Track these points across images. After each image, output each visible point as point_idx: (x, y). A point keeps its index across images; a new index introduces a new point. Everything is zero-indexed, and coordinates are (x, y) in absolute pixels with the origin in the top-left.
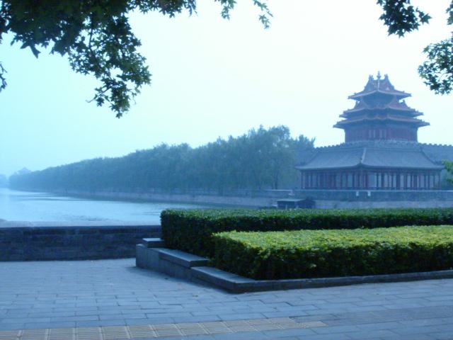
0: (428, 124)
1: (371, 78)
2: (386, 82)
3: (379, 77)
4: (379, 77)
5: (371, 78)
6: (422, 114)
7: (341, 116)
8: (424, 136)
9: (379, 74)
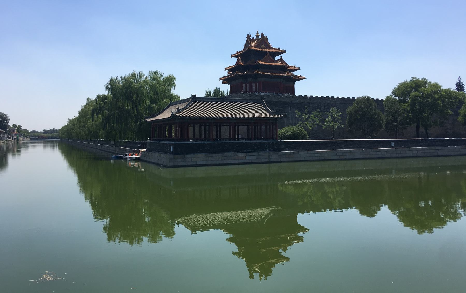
0: (305, 78)
1: (249, 37)
2: (263, 41)
3: (257, 36)
6: (299, 69)
8: (301, 89)
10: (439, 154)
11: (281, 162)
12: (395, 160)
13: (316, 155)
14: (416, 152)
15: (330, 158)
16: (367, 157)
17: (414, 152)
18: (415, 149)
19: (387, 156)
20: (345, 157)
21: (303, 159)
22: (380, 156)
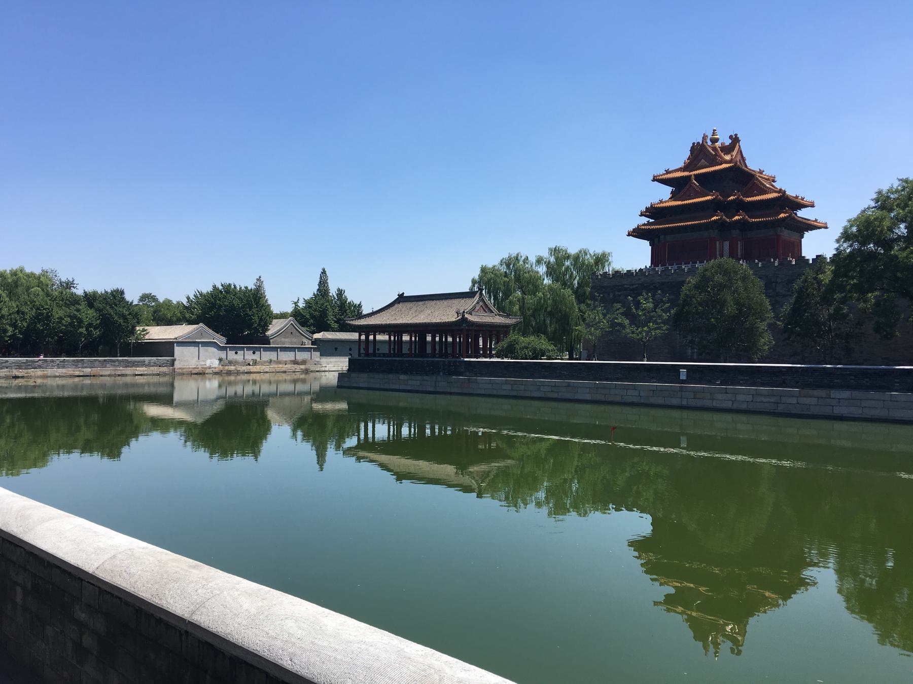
10: (838, 411)
11: (451, 393)
12: (676, 414)
13: (505, 387)
14: (749, 398)
15: (528, 394)
16: (602, 398)
17: (741, 397)
18: (744, 392)
19: (653, 400)
20: (555, 395)
21: (482, 392)
22: (635, 400)
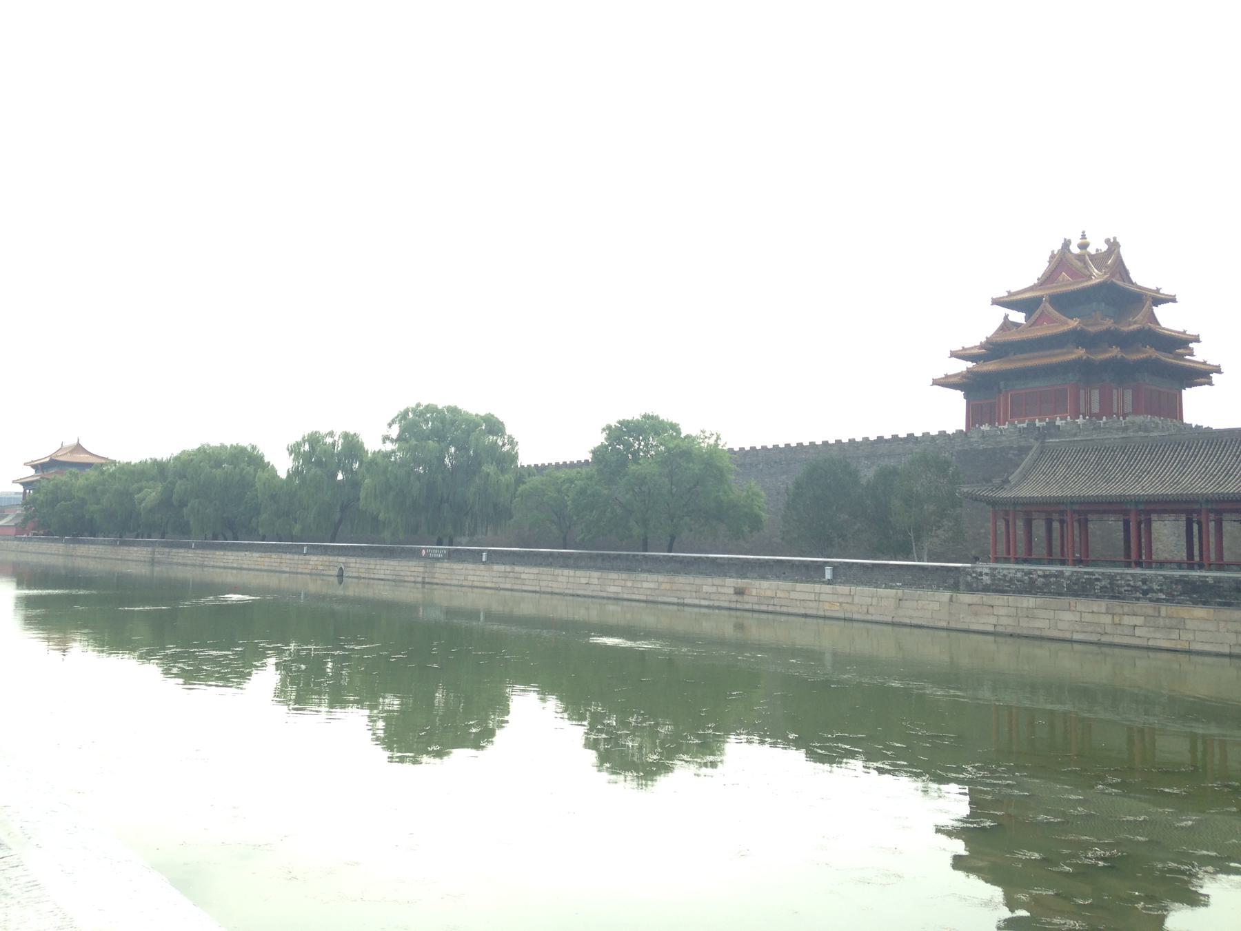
1: (1067, 244)
3: (1083, 246)
4: (1083, 246)
5: (1067, 244)
7: (954, 355)
9: (1084, 237)
